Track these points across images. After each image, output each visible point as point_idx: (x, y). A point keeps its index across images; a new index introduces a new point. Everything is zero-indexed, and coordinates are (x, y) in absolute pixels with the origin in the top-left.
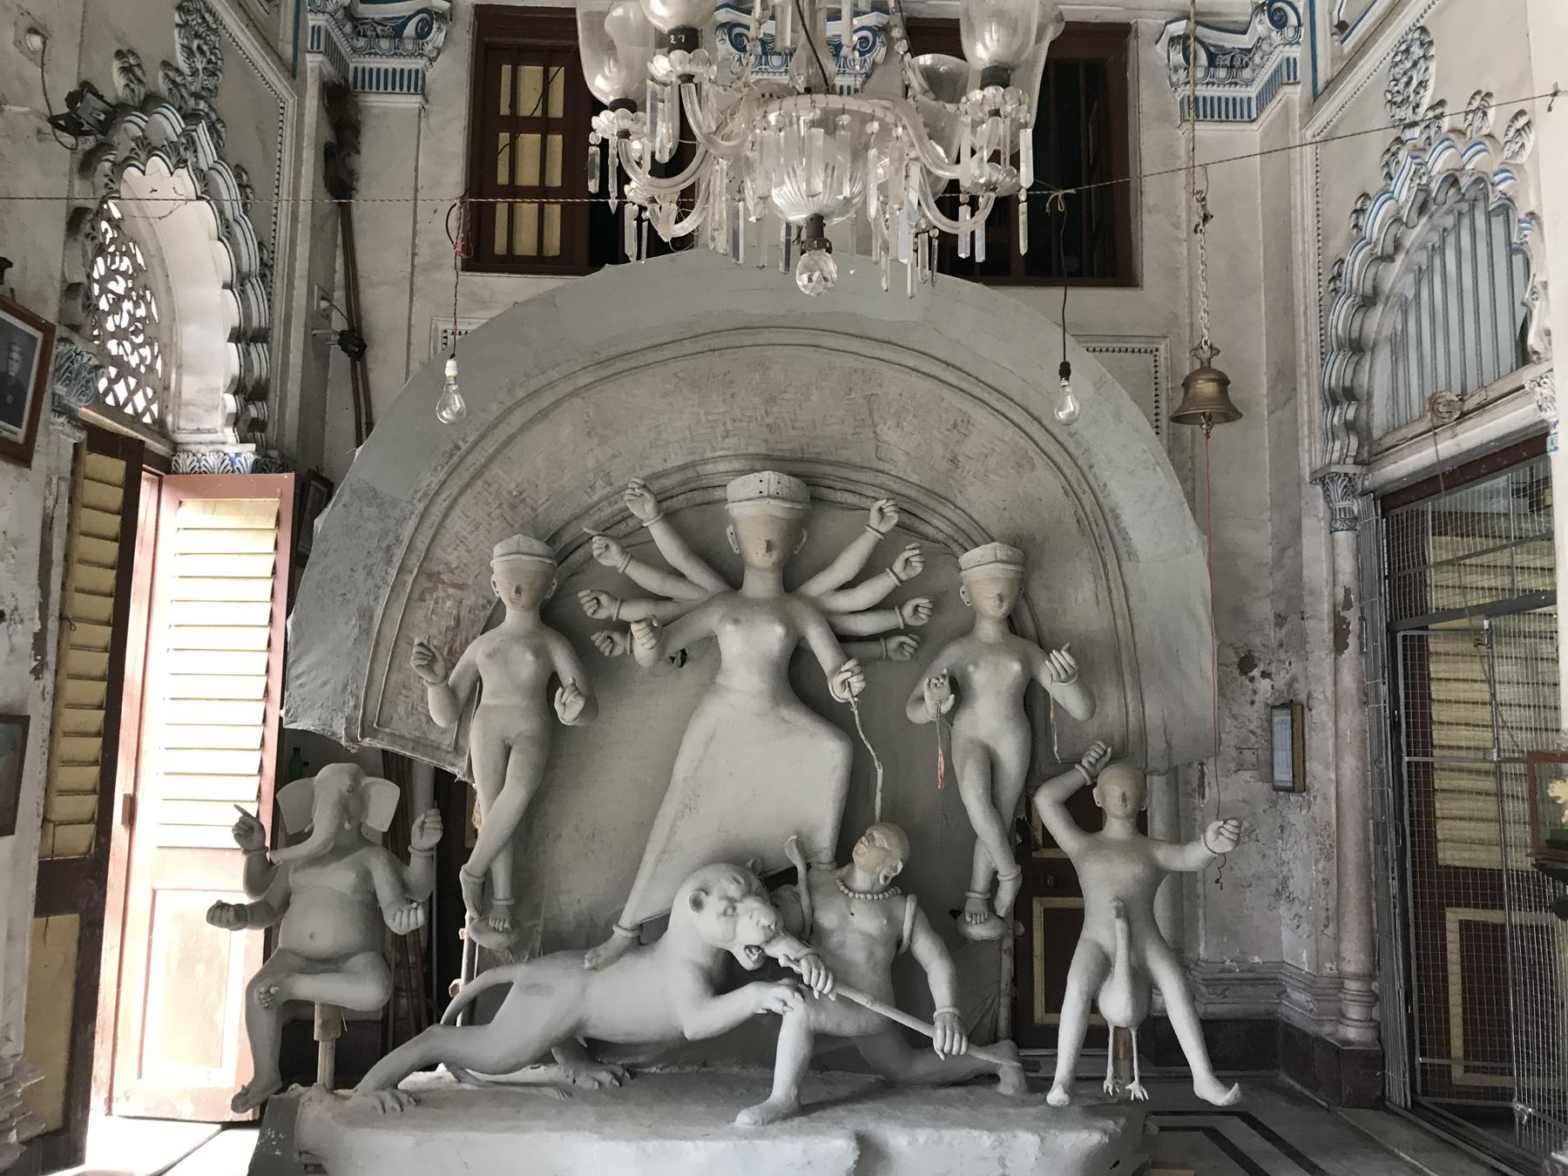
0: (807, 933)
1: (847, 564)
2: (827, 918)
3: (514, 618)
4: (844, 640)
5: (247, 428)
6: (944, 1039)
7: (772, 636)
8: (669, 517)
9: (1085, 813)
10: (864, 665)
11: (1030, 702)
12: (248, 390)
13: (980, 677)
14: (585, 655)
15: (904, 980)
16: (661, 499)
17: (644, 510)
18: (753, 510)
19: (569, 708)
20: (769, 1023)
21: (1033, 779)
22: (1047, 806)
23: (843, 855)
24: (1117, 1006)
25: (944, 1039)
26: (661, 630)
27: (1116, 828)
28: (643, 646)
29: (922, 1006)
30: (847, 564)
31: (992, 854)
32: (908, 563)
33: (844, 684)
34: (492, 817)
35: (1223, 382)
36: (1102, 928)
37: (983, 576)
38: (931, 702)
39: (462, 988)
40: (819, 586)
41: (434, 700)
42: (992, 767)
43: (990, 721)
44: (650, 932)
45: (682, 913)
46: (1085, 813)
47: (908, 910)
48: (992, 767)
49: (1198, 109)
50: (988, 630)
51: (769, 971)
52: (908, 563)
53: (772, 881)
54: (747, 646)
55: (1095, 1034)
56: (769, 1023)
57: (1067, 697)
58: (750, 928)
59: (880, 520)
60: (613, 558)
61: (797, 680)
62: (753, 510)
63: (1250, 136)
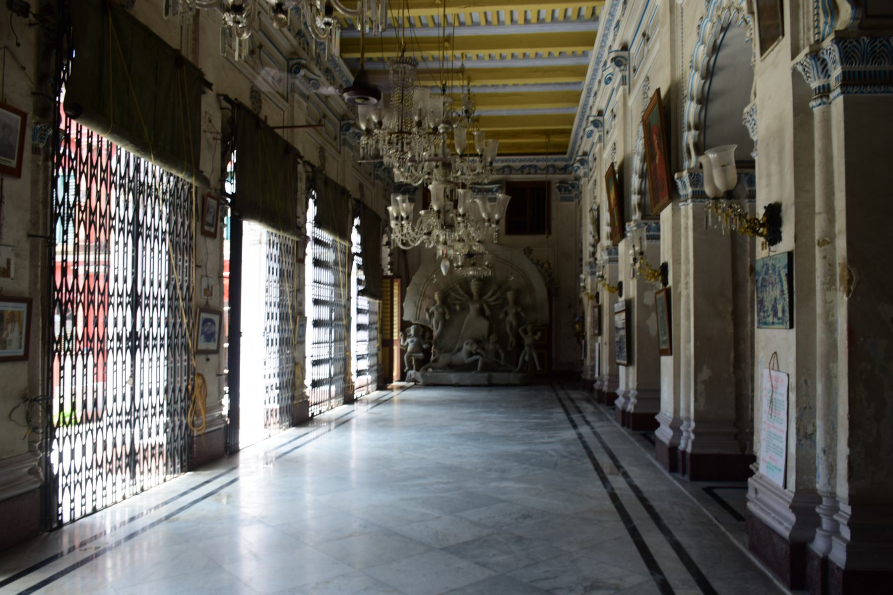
0: (483, 349)
1: (489, 294)
2: (486, 346)
3: (438, 303)
4: (489, 306)
5: (391, 270)
6: (502, 362)
7: (477, 306)
8: (461, 287)
9: (525, 332)
10: (491, 311)
11: (517, 315)
12: (391, 263)
13: (509, 311)
14: (449, 309)
15: (497, 355)
16: (460, 284)
17: (458, 286)
18: (474, 287)
19: (447, 317)
20: (477, 361)
21: (519, 326)
22: (520, 330)
23: (488, 338)
24: (527, 358)
25: (502, 362)
26: (460, 306)
27: (529, 334)
28: (458, 308)
29: (500, 359)
30: (489, 294)
31: (511, 338)
32: (499, 294)
33: (488, 313)
34: (436, 333)
35: (549, 264)
36: (526, 349)
37: (510, 295)
38: (501, 316)
39: (432, 358)
40: (485, 297)
41: (427, 316)
42: (511, 325)
43: (510, 318)
44: (460, 349)
45: (465, 346)
46: (525, 332)
47: (498, 346)
48: (511, 325)
49: (564, 199)
50: (511, 304)
51: (477, 354)
52: (499, 294)
53: (478, 341)
54: (473, 308)
55: (524, 360)
56: (477, 361)
57: (522, 314)
58: (475, 347)
59: (494, 287)
60: (453, 294)
61: (481, 312)
62: (474, 287)
63: (574, 203)
